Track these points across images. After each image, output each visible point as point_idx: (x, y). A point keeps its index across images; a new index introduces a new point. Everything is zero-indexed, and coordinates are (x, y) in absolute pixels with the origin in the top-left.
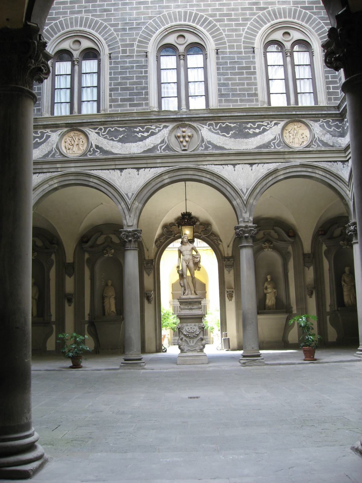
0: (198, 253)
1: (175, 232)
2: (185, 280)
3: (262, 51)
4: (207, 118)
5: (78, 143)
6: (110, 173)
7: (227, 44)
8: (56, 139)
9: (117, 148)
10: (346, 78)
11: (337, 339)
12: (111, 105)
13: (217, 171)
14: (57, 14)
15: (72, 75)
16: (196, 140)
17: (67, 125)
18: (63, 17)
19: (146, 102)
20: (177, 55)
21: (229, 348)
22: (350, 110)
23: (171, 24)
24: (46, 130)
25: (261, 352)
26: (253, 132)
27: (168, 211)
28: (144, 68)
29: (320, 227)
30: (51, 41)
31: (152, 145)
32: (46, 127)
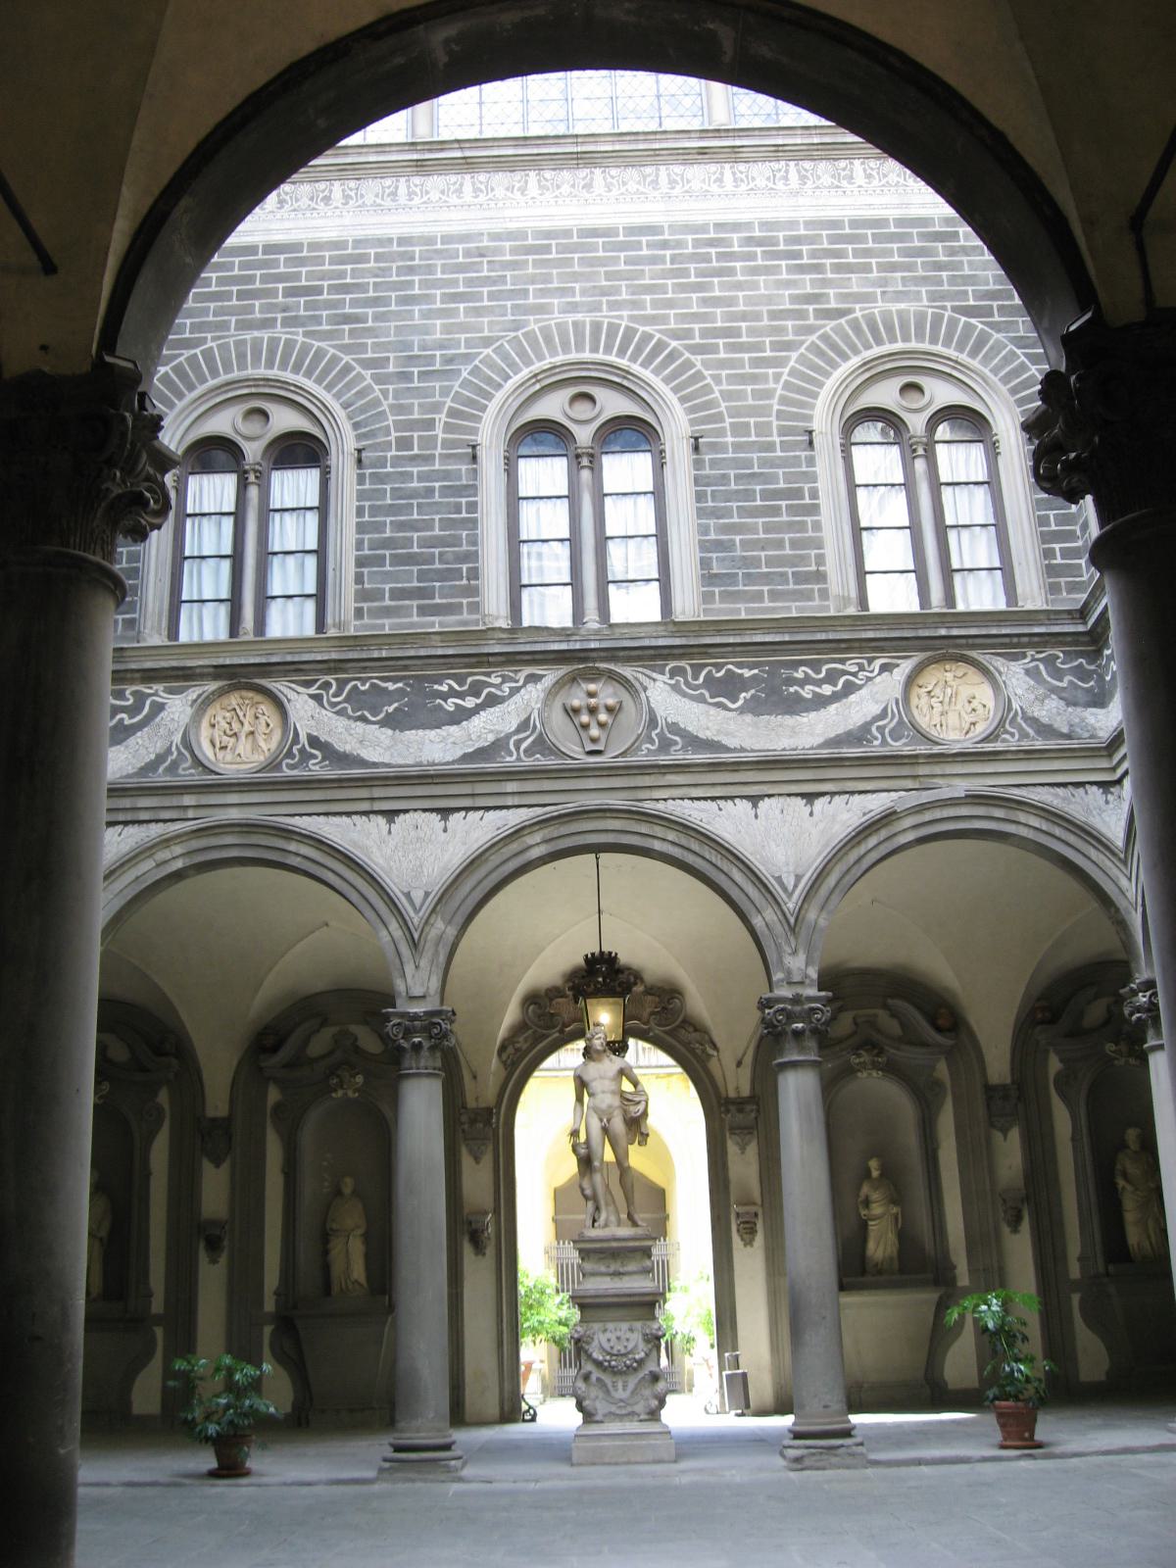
0: (639, 1088)
1: (565, 1016)
2: (598, 1178)
3: (838, 441)
4: (666, 652)
7: (728, 420)
8: (182, 716)
10: (1102, 522)
11: (1107, 1373)
12: (362, 608)
14: (195, 328)
15: (239, 516)
16: (631, 721)
17: (218, 672)
18: (214, 339)
19: (470, 600)
20: (571, 454)
21: (746, 1407)
22: (1119, 624)
23: (553, 360)
24: (151, 688)
25: (856, 1419)
26: (815, 693)
27: (543, 949)
28: (464, 493)
29: (1039, 999)
30: (176, 410)
31: (491, 738)
32: (150, 676)
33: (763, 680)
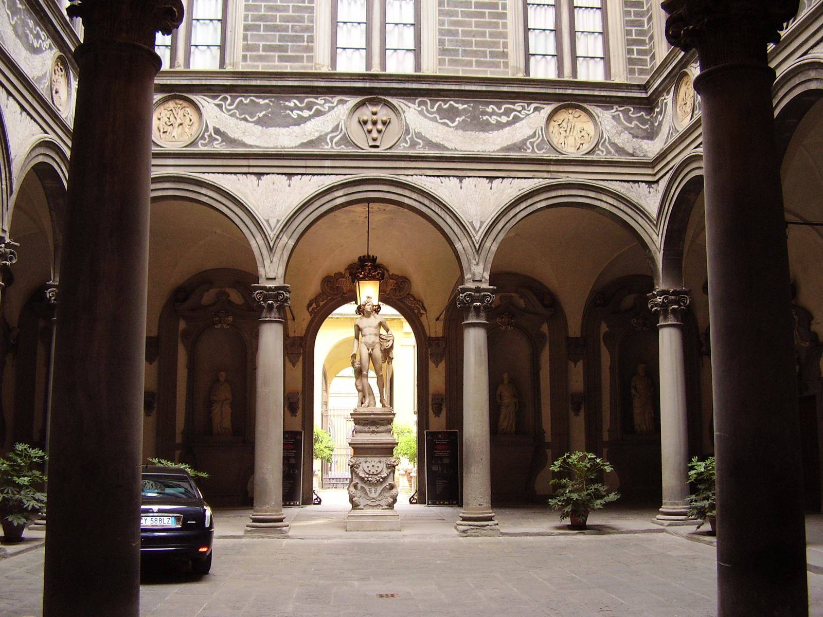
5: (181, 122)
6: (239, 180)
9: (253, 135)
12: (246, 55)
13: (431, 188)
16: (394, 130)
19: (308, 54)
26: (496, 120)
31: (317, 135)
33: (470, 111)
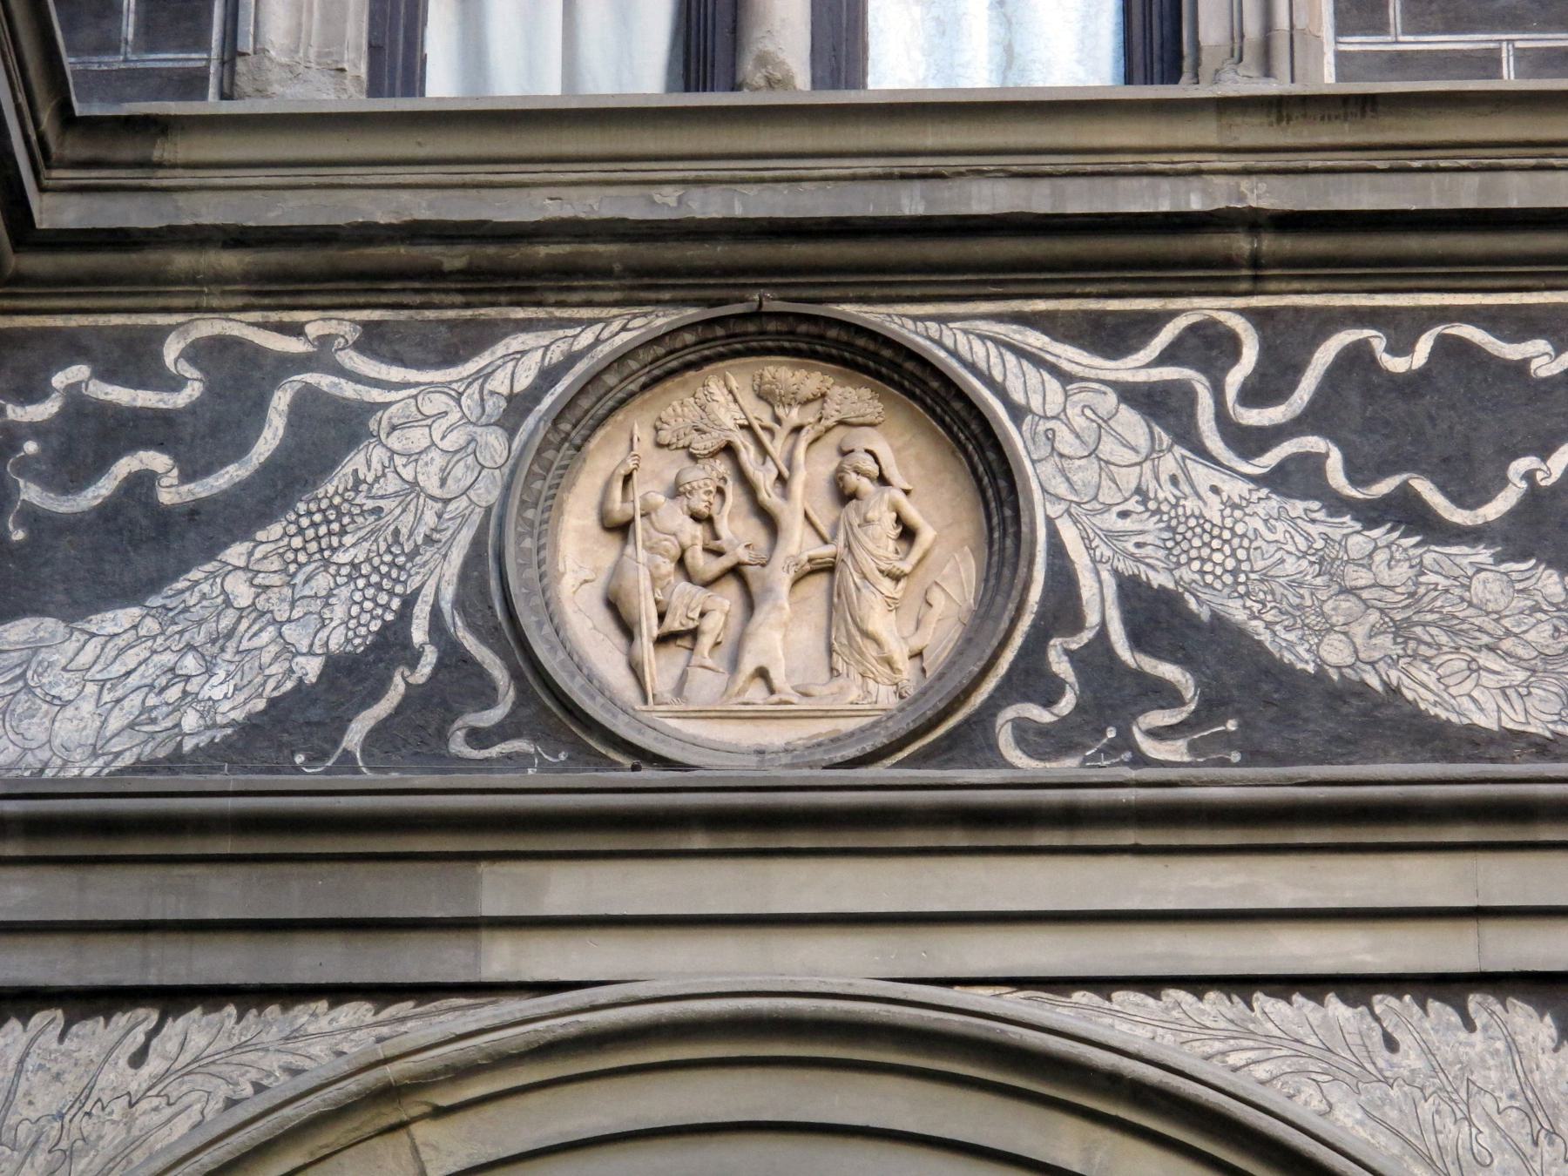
6: (1391, 1044)
24: (296, 330)
